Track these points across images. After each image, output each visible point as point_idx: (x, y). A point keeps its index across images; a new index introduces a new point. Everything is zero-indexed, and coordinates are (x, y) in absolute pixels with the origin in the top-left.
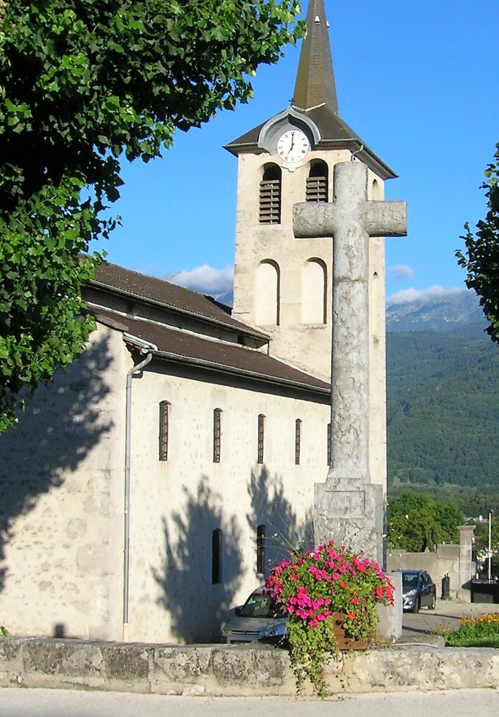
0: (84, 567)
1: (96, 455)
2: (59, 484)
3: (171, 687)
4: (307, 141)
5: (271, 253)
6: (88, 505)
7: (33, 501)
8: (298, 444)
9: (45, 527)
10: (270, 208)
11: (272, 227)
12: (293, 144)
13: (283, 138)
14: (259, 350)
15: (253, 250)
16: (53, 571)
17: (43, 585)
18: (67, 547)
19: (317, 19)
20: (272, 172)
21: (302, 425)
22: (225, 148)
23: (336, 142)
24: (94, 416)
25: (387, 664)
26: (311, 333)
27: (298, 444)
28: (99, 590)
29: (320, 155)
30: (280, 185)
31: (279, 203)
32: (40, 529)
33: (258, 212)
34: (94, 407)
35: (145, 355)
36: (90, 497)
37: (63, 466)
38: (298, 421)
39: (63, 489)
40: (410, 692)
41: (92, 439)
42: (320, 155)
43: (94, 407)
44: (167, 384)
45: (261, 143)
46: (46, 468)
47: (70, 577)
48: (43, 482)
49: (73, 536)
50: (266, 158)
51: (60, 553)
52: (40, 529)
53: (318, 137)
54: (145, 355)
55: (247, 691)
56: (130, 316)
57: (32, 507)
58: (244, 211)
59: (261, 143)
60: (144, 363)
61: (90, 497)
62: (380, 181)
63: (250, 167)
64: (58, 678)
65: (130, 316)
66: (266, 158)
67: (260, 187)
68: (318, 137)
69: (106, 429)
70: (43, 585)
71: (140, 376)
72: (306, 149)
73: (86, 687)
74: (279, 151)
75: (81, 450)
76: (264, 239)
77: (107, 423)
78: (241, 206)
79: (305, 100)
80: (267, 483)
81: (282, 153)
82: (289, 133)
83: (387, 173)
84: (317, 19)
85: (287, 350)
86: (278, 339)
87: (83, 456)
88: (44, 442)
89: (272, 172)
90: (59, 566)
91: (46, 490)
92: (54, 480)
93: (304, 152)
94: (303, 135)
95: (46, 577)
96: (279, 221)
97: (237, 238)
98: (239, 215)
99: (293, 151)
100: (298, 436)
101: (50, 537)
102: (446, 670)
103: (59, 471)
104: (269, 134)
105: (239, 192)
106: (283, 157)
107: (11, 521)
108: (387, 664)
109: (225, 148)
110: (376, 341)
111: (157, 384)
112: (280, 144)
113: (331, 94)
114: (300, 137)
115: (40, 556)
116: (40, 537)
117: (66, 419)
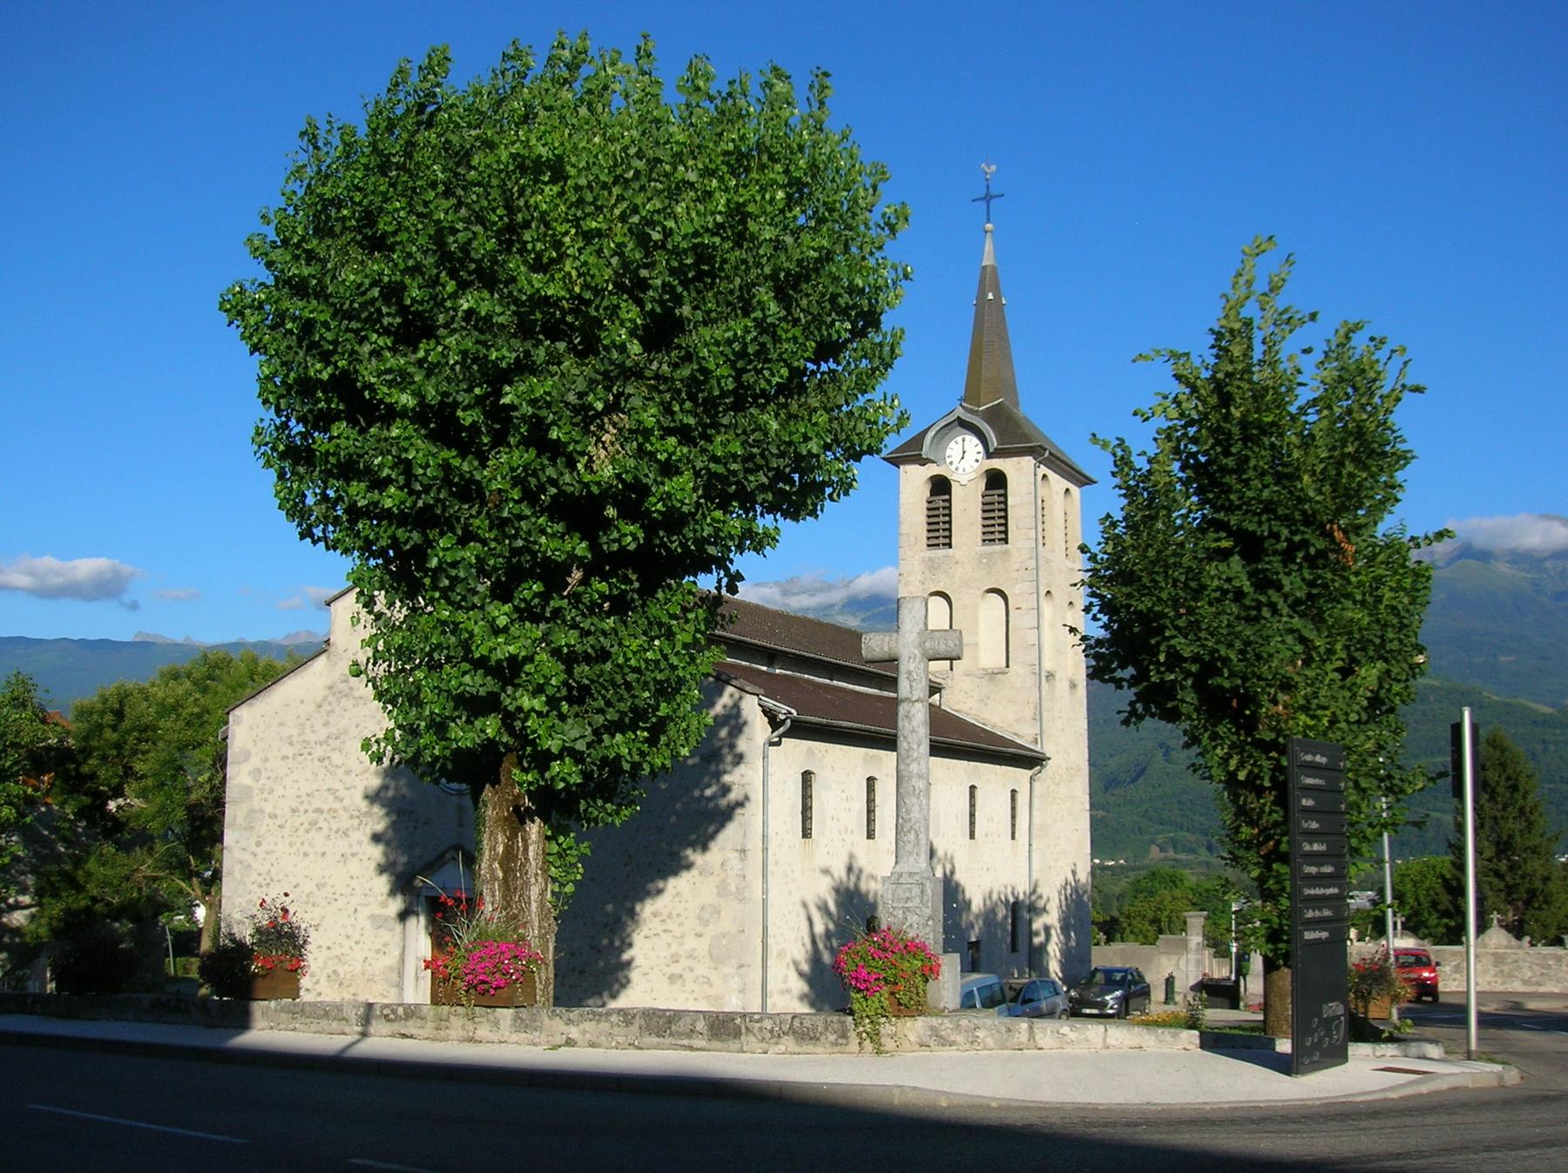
0: (716, 959)
1: (728, 836)
2: (689, 866)
3: (759, 1046)
4: (980, 448)
6: (722, 889)
7: (661, 884)
8: (972, 815)
9: (675, 913)
10: (940, 530)
11: (941, 552)
16: (684, 963)
17: (673, 978)
18: (699, 935)
19: (990, 296)
20: (941, 486)
21: (978, 793)
24: (726, 790)
25: (932, 1028)
27: (972, 815)
28: (735, 983)
29: (997, 463)
30: (950, 501)
31: (950, 522)
32: (670, 916)
33: (925, 534)
34: (727, 778)
35: (783, 722)
36: (724, 880)
37: (693, 845)
38: (973, 788)
39: (694, 871)
40: (951, 1052)
41: (724, 816)
42: (997, 463)
43: (727, 778)
44: (810, 751)
45: (925, 453)
46: (675, 848)
47: (701, 969)
48: (674, 865)
49: (706, 923)
51: (691, 943)
52: (670, 916)
53: (994, 443)
54: (783, 722)
55: (820, 1050)
56: (771, 670)
57: (660, 892)
59: (926, 452)
60: (782, 730)
61: (724, 880)
62: (1075, 490)
63: (914, 481)
64: (668, 1040)
65: (771, 670)
67: (926, 505)
68: (994, 443)
69: (740, 804)
70: (673, 978)
71: (778, 744)
72: (980, 457)
73: (691, 1048)
75: (711, 829)
76: (932, 566)
77: (741, 798)
78: (904, 528)
82: (959, 439)
84: (990, 296)
87: (712, 837)
88: (673, 819)
89: (941, 486)
90: (690, 956)
91: (675, 873)
92: (684, 862)
94: (976, 441)
95: (676, 969)
96: (950, 545)
98: (902, 539)
99: (964, 459)
100: (972, 805)
101: (681, 924)
102: (981, 1034)
103: (689, 852)
105: (902, 511)
107: (638, 908)
108: (932, 1028)
110: (1073, 686)
111: (798, 751)
112: (948, 452)
113: (1010, 387)
114: (972, 442)
115: (669, 945)
116: (670, 925)
117: (697, 793)
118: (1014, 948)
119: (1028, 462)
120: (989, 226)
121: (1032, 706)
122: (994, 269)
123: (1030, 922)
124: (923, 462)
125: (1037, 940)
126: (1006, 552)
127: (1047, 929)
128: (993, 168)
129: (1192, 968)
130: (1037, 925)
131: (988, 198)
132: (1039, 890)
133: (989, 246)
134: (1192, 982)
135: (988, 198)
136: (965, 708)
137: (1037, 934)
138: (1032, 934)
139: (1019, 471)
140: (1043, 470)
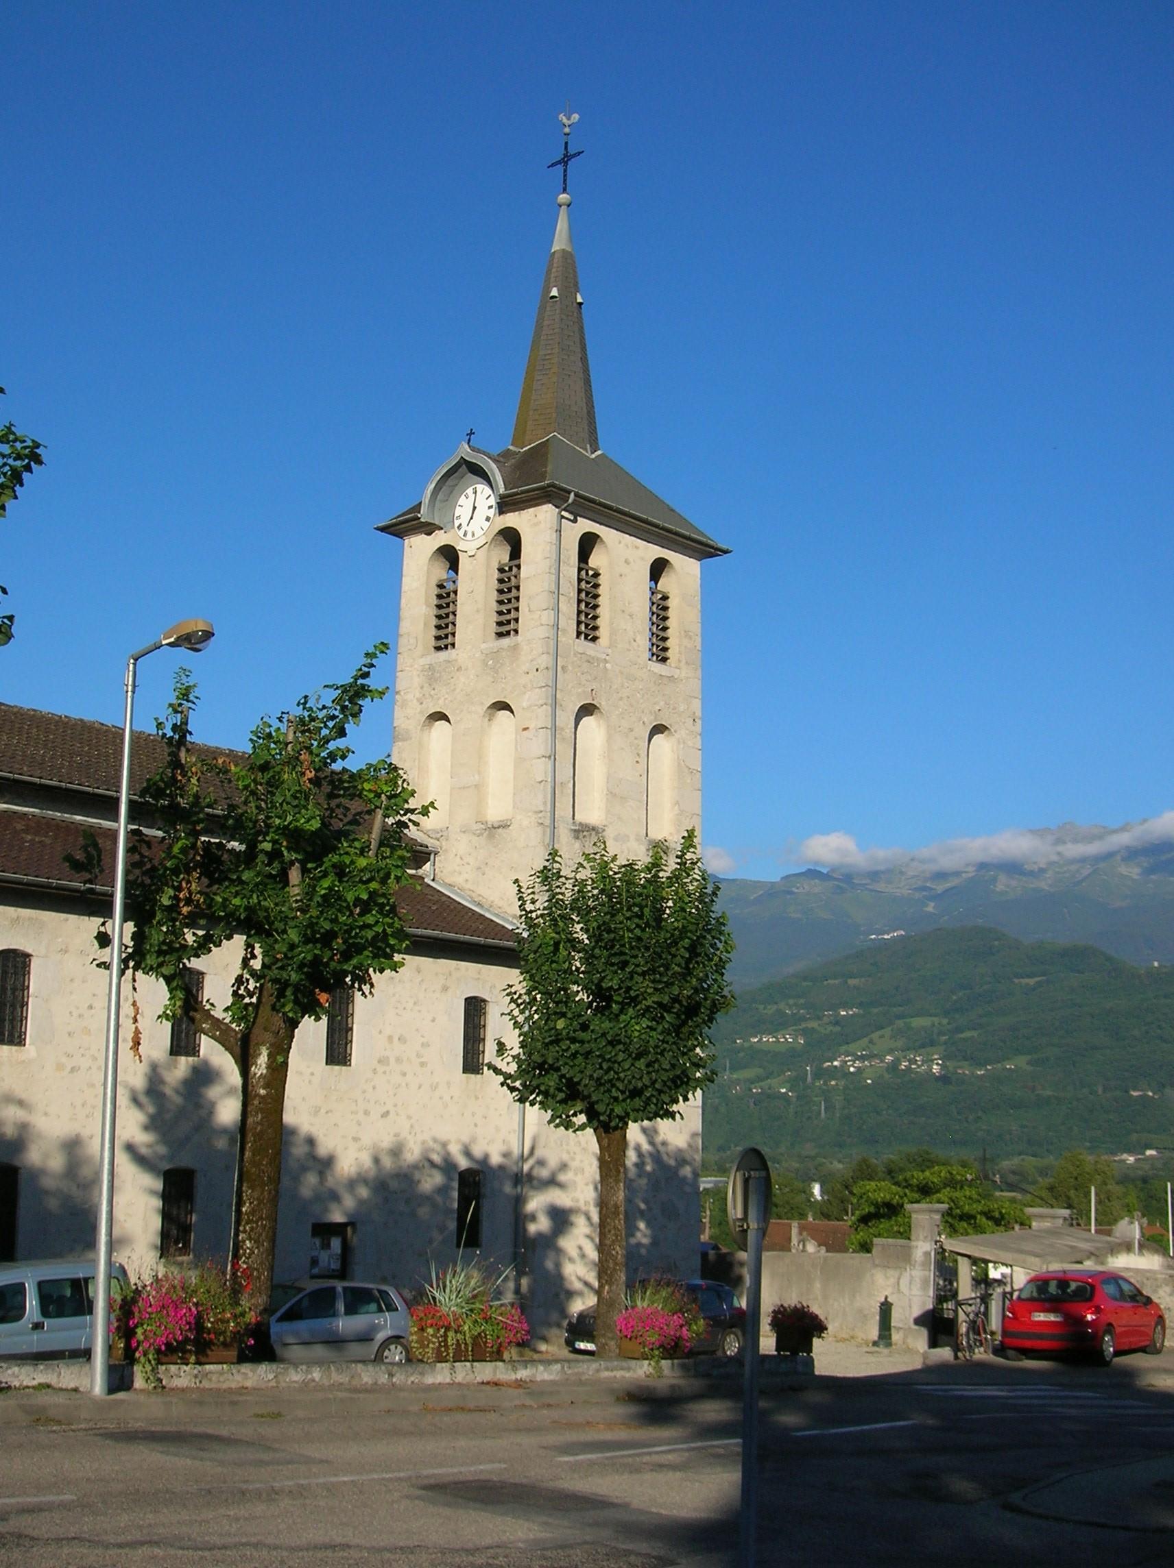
5: (441, 702)
12: (475, 508)
13: (462, 500)
14: (420, 872)
15: (418, 700)
19: (554, 292)
22: (382, 529)
23: (523, 492)
26: (491, 837)
29: (512, 520)
45: (424, 515)
58: (408, 634)
59: (424, 515)
74: (457, 523)
76: (432, 676)
80: (213, 1092)
81: (460, 527)
82: (470, 491)
83: (703, 550)
85: (457, 868)
86: (446, 850)
93: (488, 519)
97: (398, 681)
104: (441, 496)
105: (403, 601)
106: (461, 533)
109: (382, 529)
112: (458, 511)
119: (546, 513)
120: (563, 197)
123: (519, 1201)
124: (429, 528)
125: (532, 1228)
126: (515, 648)
127: (561, 1218)
128: (575, 117)
129: (916, 1291)
130: (536, 1203)
131: (566, 159)
132: (539, 1153)
133: (562, 225)
134: (917, 1312)
135: (566, 159)
136: (458, 880)
137: (533, 1218)
138: (520, 1219)
139: (539, 525)
140: (587, 525)
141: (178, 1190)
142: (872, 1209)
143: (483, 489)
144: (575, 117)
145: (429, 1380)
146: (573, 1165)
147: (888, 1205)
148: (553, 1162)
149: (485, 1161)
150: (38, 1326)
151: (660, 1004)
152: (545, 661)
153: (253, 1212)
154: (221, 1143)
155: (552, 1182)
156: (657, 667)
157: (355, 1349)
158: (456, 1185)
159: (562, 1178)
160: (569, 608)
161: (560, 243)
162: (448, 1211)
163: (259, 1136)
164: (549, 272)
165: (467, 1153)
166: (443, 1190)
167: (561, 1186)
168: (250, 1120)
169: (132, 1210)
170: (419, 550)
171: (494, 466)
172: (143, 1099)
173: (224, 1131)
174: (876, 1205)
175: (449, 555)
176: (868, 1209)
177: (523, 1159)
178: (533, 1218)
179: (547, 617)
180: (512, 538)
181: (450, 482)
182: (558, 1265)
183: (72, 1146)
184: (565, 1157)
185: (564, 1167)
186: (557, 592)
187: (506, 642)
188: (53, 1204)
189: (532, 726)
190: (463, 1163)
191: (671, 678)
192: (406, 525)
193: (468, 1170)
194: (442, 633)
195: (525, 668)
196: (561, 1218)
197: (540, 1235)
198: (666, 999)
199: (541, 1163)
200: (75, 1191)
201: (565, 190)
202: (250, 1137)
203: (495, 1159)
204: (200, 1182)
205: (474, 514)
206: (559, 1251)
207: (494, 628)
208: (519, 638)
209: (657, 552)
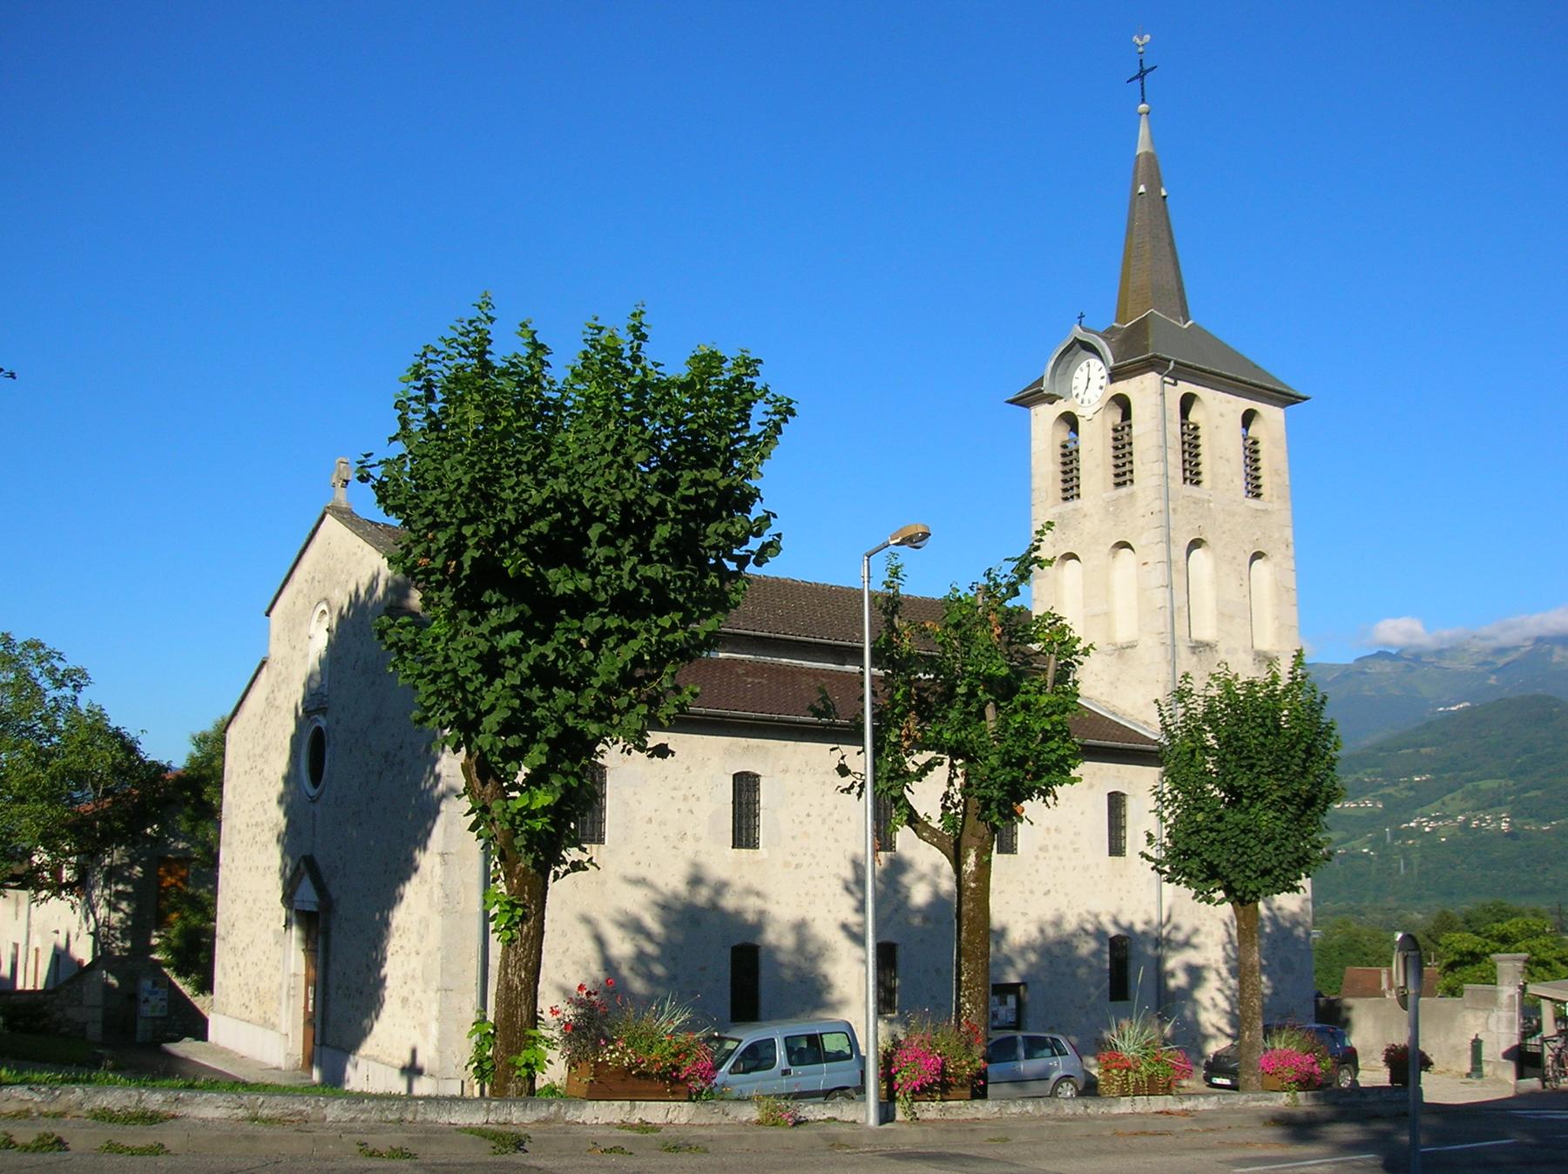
19: (1142, 189)
26: (1120, 656)
29: (1121, 387)
50: (1061, 407)
66: (1061, 407)
79: (1125, 312)
80: (907, 879)
82: (1084, 365)
83: (1284, 398)
98: (1035, 495)
109: (1012, 402)
112: (1075, 383)
118: (1119, 988)
119: (1151, 379)
120: (1143, 107)
121: (1161, 686)
122: (1150, 157)
123: (1160, 961)
124: (1051, 399)
125: (1172, 983)
126: (1131, 495)
127: (1196, 974)
128: (1147, 38)
129: (1503, 1030)
130: (1174, 962)
131: (1142, 75)
132: (1174, 919)
133: (1144, 131)
134: (1504, 1047)
135: (1142, 75)
137: (1172, 974)
138: (1161, 976)
139: (1144, 390)
140: (1185, 387)
141: (887, 957)
142: (1457, 958)
143: (1095, 362)
144: (1147, 38)
145: (1115, 1111)
146: (1204, 929)
147: (1471, 953)
148: (1187, 927)
149: (1130, 929)
150: (786, 1073)
151: (1283, 798)
152: (1157, 505)
153: (970, 980)
154: (917, 921)
155: (1187, 944)
156: (1253, 503)
157: (1035, 1087)
158: (1107, 949)
159: (1195, 940)
160: (1175, 459)
161: (1143, 147)
162: (1102, 971)
163: (972, 920)
164: (1135, 172)
165: (1116, 923)
166: (1096, 954)
167: (1195, 947)
168: (964, 908)
169: (851, 977)
170: (1044, 417)
171: (1103, 343)
172: (853, 887)
173: (919, 910)
174: (1461, 954)
175: (1070, 420)
176: (1453, 957)
177: (1161, 925)
178: (1172, 974)
179: (1158, 468)
180: (1123, 404)
181: (1067, 358)
182: (1195, 1014)
183: (800, 927)
184: (1197, 923)
185: (1196, 931)
186: (1164, 446)
187: (1123, 491)
188: (787, 974)
189: (1150, 560)
190: (1113, 931)
191: (1265, 511)
192: (1031, 397)
193: (1117, 936)
194: (1068, 486)
195: (1141, 512)
196: (1196, 974)
197: (1179, 988)
198: (1288, 794)
199: (1177, 928)
200: (805, 965)
201: (1143, 101)
202: (965, 921)
203: (1139, 927)
204: (901, 954)
205: (1089, 385)
206: (1195, 1002)
207: (1112, 480)
208: (1135, 487)
209: (1246, 404)
